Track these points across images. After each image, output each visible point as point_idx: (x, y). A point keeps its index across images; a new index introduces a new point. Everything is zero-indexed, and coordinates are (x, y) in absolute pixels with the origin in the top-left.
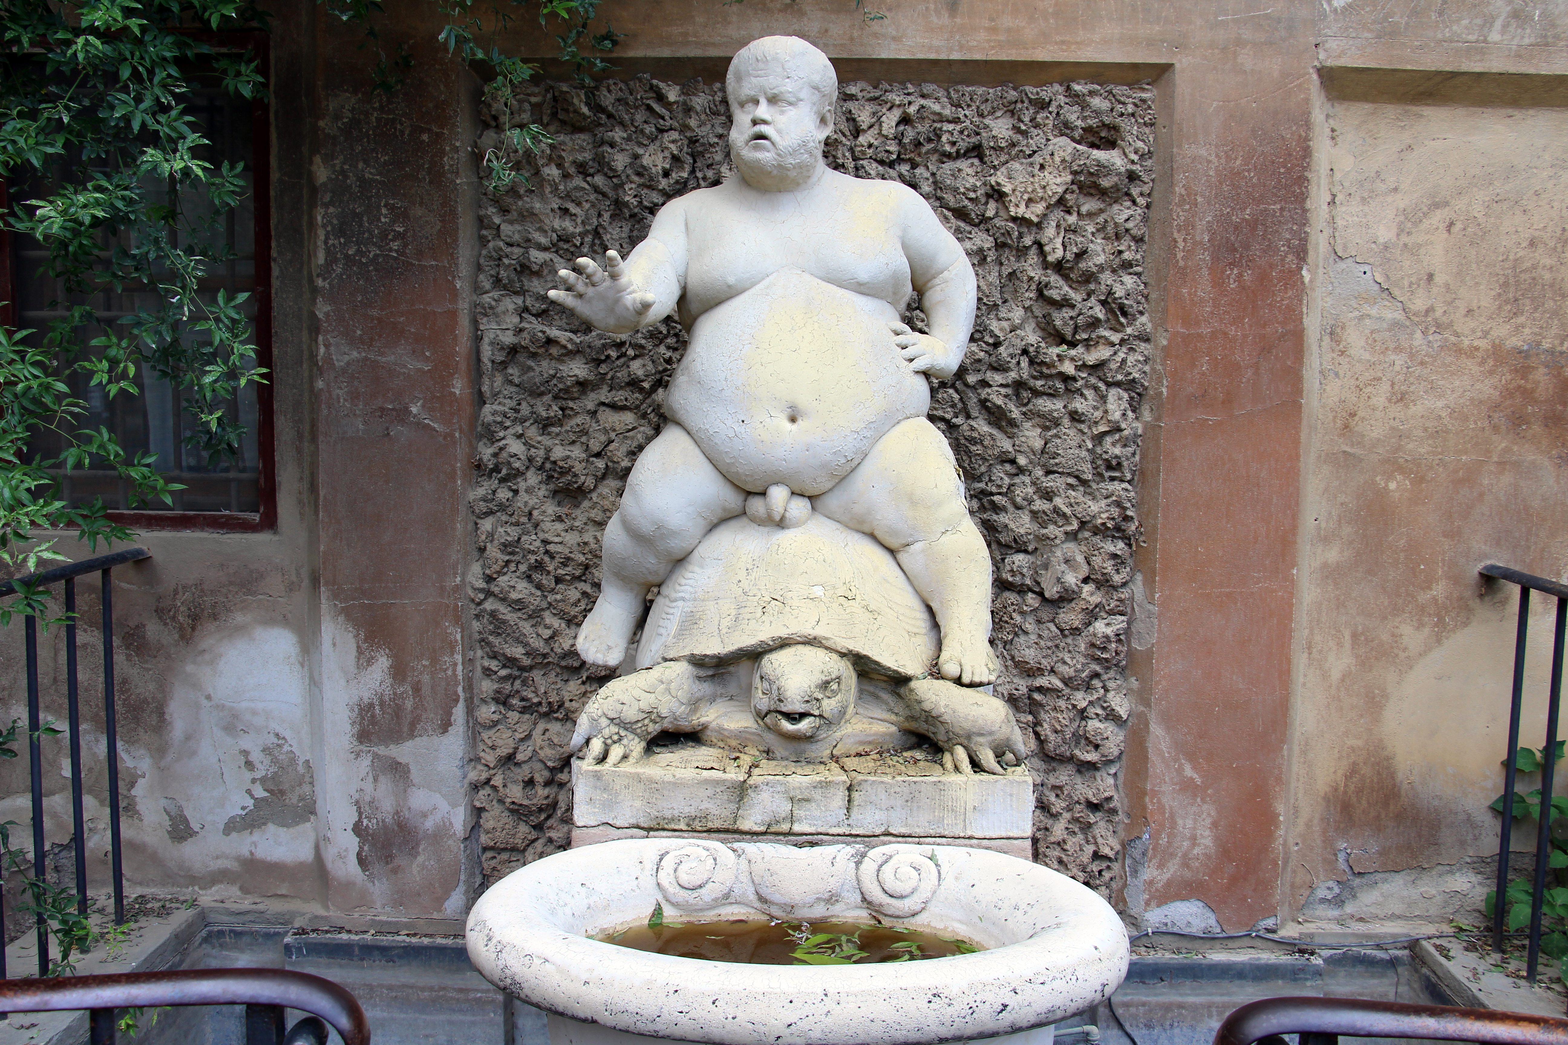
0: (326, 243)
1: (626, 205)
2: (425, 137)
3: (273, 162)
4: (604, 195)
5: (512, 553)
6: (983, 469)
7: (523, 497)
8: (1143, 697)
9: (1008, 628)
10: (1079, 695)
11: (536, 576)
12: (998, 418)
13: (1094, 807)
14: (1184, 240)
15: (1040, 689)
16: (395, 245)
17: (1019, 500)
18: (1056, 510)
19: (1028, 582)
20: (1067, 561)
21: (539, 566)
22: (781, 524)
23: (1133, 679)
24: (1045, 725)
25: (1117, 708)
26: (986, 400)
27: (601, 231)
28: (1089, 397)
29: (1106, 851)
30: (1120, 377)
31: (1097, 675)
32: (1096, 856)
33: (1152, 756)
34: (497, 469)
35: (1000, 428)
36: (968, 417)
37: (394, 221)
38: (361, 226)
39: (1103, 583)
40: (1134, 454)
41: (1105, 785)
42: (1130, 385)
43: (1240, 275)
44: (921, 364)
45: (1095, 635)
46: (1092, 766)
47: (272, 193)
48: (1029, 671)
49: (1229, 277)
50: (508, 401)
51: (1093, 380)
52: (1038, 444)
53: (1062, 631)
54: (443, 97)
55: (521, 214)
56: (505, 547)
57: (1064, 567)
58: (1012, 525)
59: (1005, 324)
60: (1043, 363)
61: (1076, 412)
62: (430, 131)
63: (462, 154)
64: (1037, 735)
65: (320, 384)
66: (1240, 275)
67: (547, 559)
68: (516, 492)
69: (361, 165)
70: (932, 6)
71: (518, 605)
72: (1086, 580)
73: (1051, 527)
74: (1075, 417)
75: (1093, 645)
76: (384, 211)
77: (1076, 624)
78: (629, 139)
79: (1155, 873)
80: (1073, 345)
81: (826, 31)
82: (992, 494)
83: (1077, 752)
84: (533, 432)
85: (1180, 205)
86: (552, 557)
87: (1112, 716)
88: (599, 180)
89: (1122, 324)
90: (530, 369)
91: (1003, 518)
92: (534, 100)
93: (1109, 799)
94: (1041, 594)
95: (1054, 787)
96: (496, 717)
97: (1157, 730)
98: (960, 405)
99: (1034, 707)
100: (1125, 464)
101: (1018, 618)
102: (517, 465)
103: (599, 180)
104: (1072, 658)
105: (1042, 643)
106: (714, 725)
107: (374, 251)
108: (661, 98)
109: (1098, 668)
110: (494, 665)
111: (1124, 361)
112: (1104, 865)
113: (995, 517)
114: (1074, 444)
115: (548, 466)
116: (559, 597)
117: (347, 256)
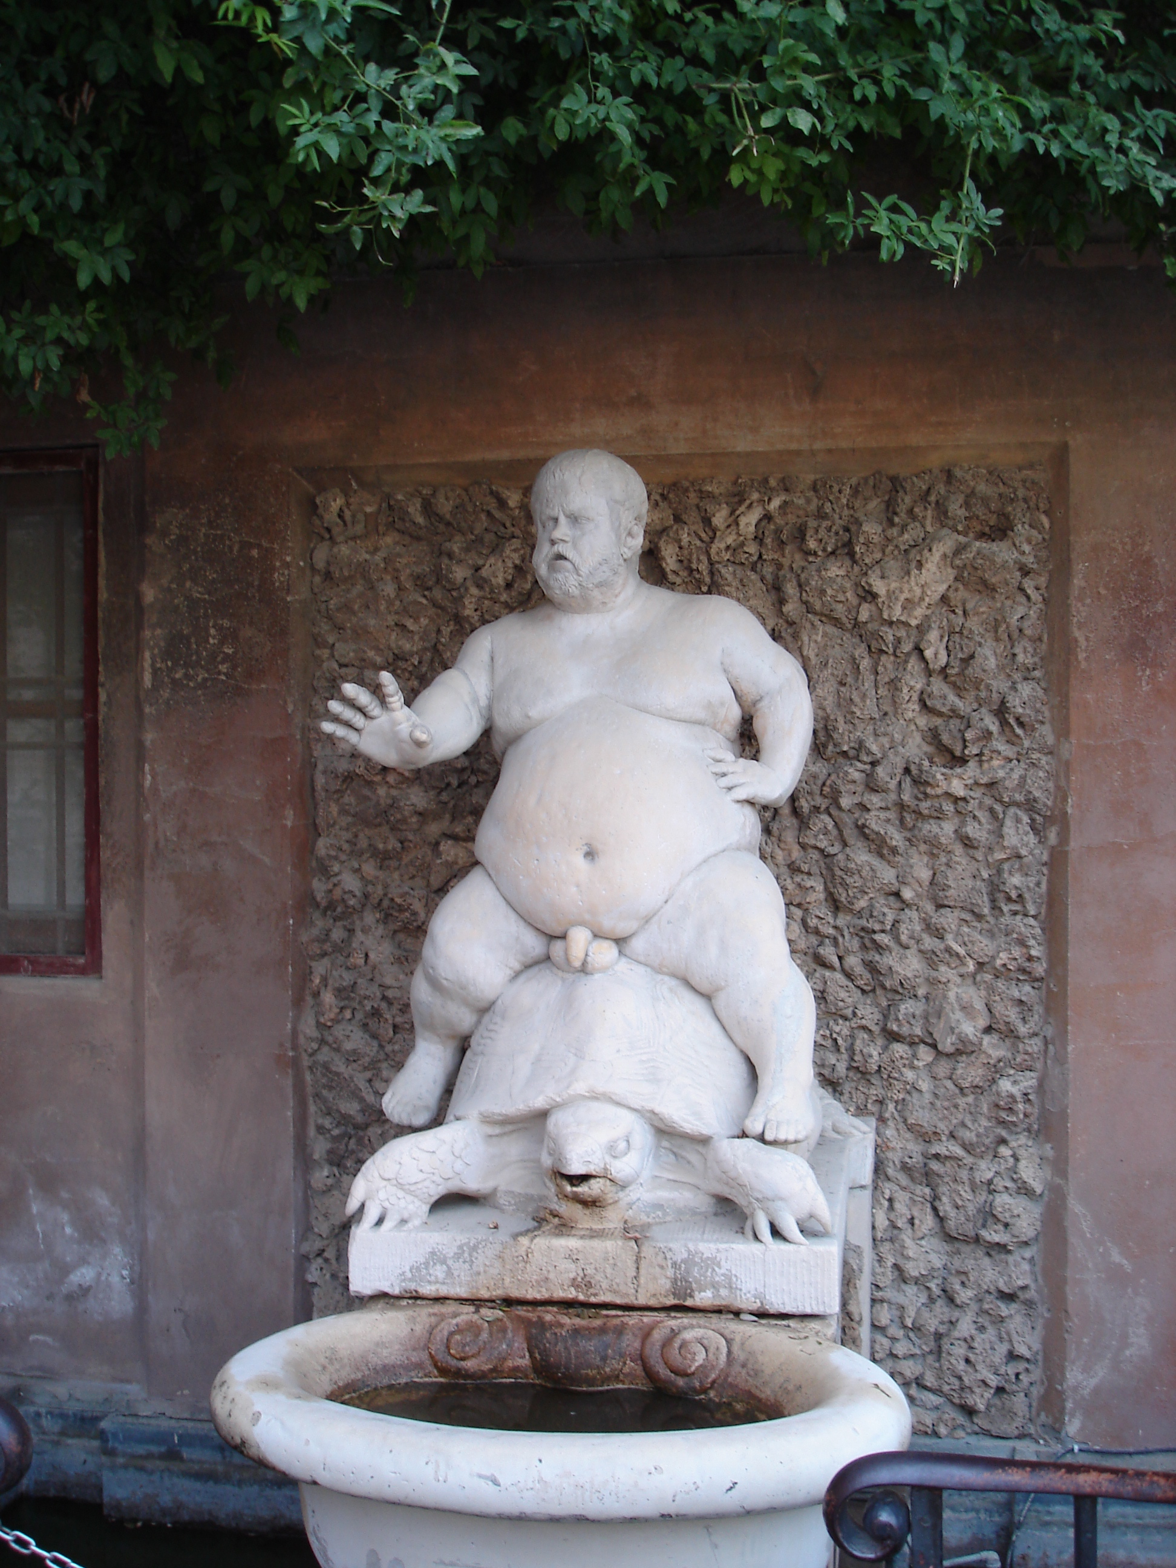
0: (153, 665)
2: (255, 553)
3: (102, 583)
4: (443, 608)
5: (348, 998)
6: (862, 903)
7: (359, 936)
8: (1059, 1165)
9: (898, 1085)
10: (983, 1164)
11: (373, 1024)
12: (880, 847)
13: (1009, 1297)
14: (1087, 639)
15: (937, 1156)
16: (223, 668)
17: (904, 938)
18: (948, 950)
19: (918, 1031)
20: (963, 1008)
21: (376, 1013)
22: (584, 969)
23: (1048, 1146)
24: (944, 1199)
25: (1030, 1181)
26: (864, 826)
27: (441, 647)
28: (983, 820)
29: (1022, 1350)
30: (1019, 797)
31: (1003, 1141)
32: (1012, 1356)
33: (1073, 1239)
34: (331, 906)
35: (881, 856)
36: (845, 844)
37: (222, 643)
38: (189, 648)
39: (1010, 1034)
40: (1038, 884)
41: (1020, 1272)
42: (1030, 805)
43: (1153, 677)
45: (998, 1094)
46: (1002, 1248)
47: (100, 615)
48: (927, 1137)
49: (1140, 678)
50: (344, 833)
51: (988, 801)
52: (925, 875)
53: (961, 1089)
54: (273, 510)
56: (339, 992)
57: (959, 1015)
58: (897, 968)
59: (885, 741)
60: (927, 783)
61: (968, 838)
62: (259, 546)
64: (935, 1209)
65: (147, 817)
66: (1153, 677)
67: (384, 1005)
68: (351, 931)
69: (188, 584)
70: (791, 392)
71: (353, 1057)
72: (988, 1030)
73: (943, 968)
74: (968, 843)
75: (997, 1106)
76: (212, 631)
77: (977, 1081)
78: (467, 550)
79: (1080, 1377)
80: (963, 761)
81: (676, 424)
82: (874, 932)
83: (983, 1233)
84: (369, 869)
85: (1080, 599)
86: (390, 1003)
87: (1024, 1190)
88: (437, 594)
89: (1018, 736)
90: (367, 798)
91: (886, 961)
92: (368, 509)
93: (1024, 1288)
94: (934, 1046)
95: (959, 1273)
96: (330, 1181)
97: (1075, 1206)
98: (835, 832)
99: (928, 1177)
100: (1026, 896)
101: (910, 1075)
102: (352, 902)
103: (437, 594)
104: (974, 1121)
105: (938, 1103)
106: (503, 1187)
107: (202, 675)
108: (502, 504)
109: (1004, 1133)
110: (327, 1122)
111: (1023, 778)
112: (1021, 1366)
113: (877, 957)
114: (968, 874)
115: (386, 903)
116: (397, 1047)
117: (174, 681)
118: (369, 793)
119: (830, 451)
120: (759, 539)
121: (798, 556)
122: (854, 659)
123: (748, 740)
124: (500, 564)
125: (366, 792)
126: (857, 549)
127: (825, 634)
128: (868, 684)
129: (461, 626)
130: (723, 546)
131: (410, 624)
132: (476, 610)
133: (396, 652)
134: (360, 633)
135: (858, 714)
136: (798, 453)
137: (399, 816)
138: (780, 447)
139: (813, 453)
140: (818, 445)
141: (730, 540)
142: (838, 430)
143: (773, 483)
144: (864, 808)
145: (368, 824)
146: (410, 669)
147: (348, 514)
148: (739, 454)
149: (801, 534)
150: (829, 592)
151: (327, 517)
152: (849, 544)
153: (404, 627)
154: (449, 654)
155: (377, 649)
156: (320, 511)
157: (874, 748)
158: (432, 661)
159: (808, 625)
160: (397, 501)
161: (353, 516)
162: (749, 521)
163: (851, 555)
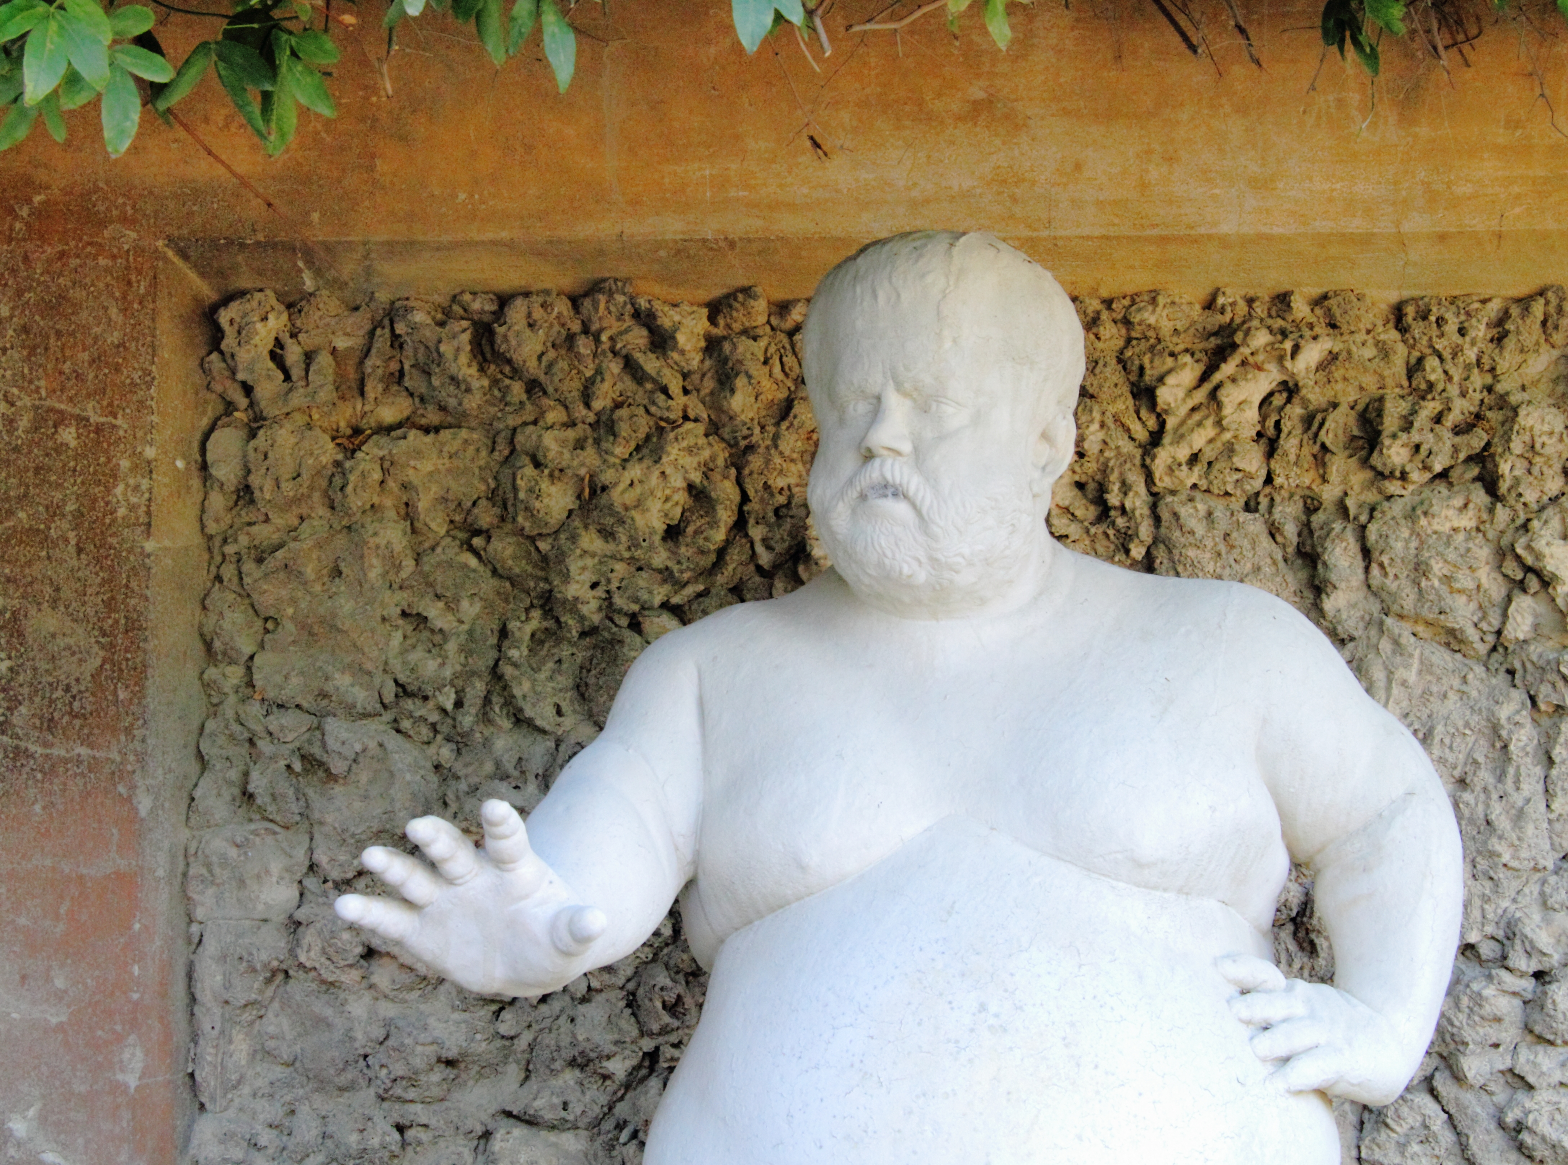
1: (573, 606)
2: (68, 435)
26: (1520, 1127)
27: (508, 671)
44: (1310, 1072)
50: (261, 1104)
54: (115, 337)
55: (305, 627)
62: (81, 420)
63: (161, 478)
70: (1354, 98)
81: (1078, 167)
90: (321, 1022)
98: (1447, 1137)
108: (661, 341)
118: (329, 1012)
119: (1442, 237)
120: (1270, 443)
121: (1359, 477)
122: (1495, 728)
123: (1300, 934)
124: (654, 478)
125: (321, 1007)
126: (1504, 468)
127: (1426, 667)
128: (1532, 786)
129: (558, 621)
130: (1183, 453)
131: (434, 611)
132: (594, 586)
133: (402, 679)
134: (317, 631)
135: (1506, 858)
136: (1365, 241)
137: (399, 1070)
138: (1323, 226)
139: (1402, 242)
140: (1417, 223)
141: (1199, 439)
142: (1465, 189)
143: (1300, 308)
144: (1519, 1081)
145: (321, 1084)
146: (434, 717)
147: (293, 354)
148: (1224, 242)
149: (1368, 435)
150: (1438, 567)
151: (243, 356)
152: (1483, 459)
153: (421, 620)
154: (526, 686)
155: (360, 671)
156: (230, 342)
157: (1544, 939)
158: (487, 700)
159: (1385, 645)
160: (414, 328)
161: (309, 357)
162: (1245, 396)
163: (1490, 483)
